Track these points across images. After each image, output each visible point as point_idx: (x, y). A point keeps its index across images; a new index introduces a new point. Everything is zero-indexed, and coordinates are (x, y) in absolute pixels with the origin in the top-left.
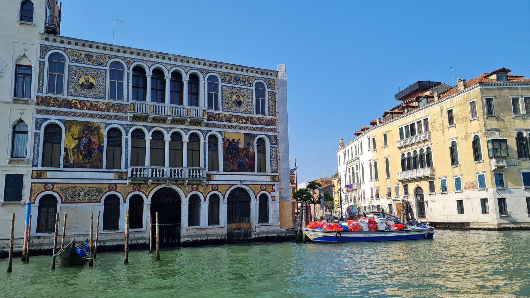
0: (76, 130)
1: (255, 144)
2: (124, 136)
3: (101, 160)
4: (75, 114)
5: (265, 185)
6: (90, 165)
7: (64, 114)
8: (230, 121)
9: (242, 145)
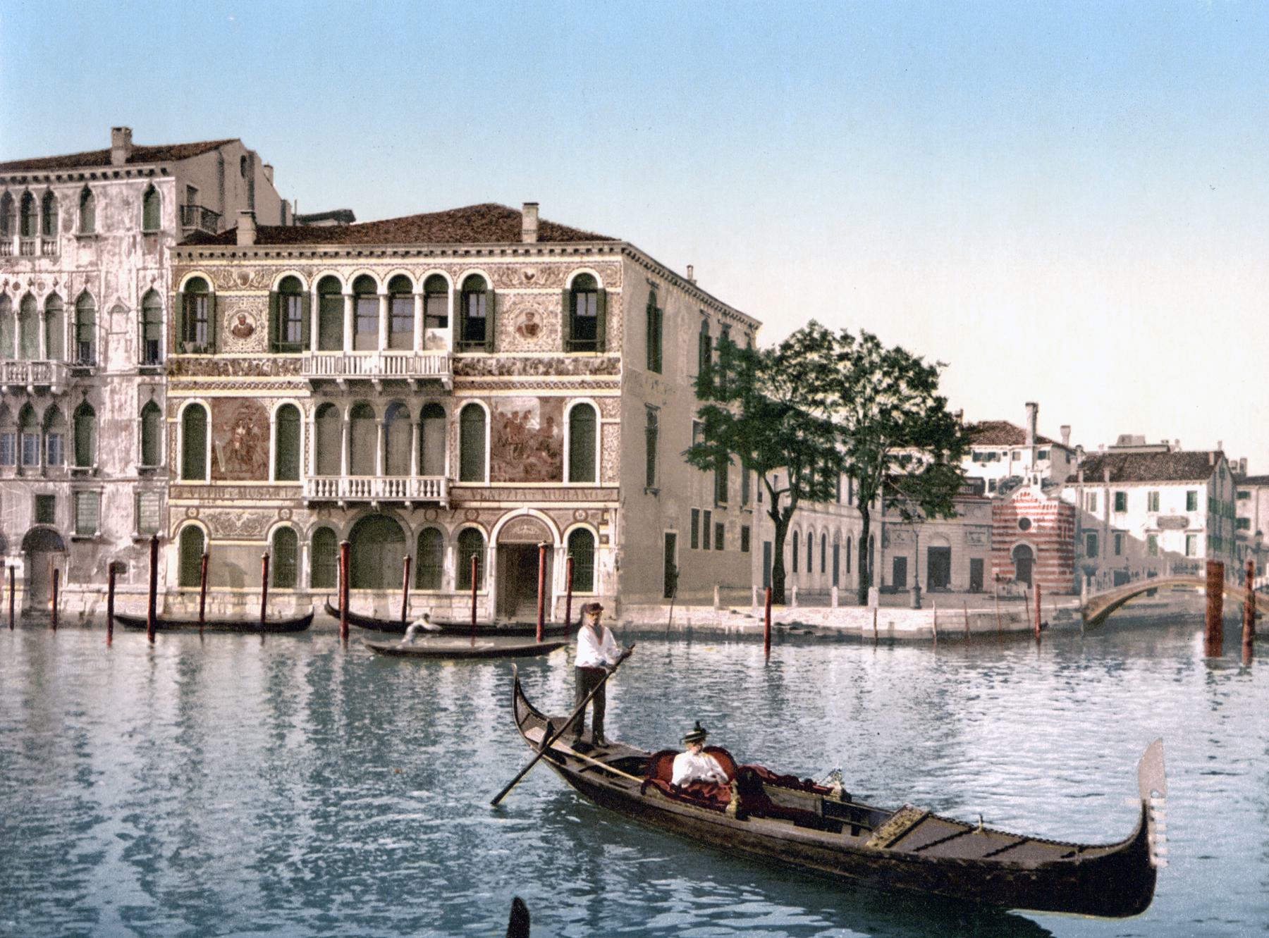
0: (230, 413)
1: (566, 418)
2: (303, 419)
3: (266, 465)
4: (225, 386)
5: (585, 510)
6: (248, 475)
7: (209, 386)
8: (510, 373)
9: (535, 424)
